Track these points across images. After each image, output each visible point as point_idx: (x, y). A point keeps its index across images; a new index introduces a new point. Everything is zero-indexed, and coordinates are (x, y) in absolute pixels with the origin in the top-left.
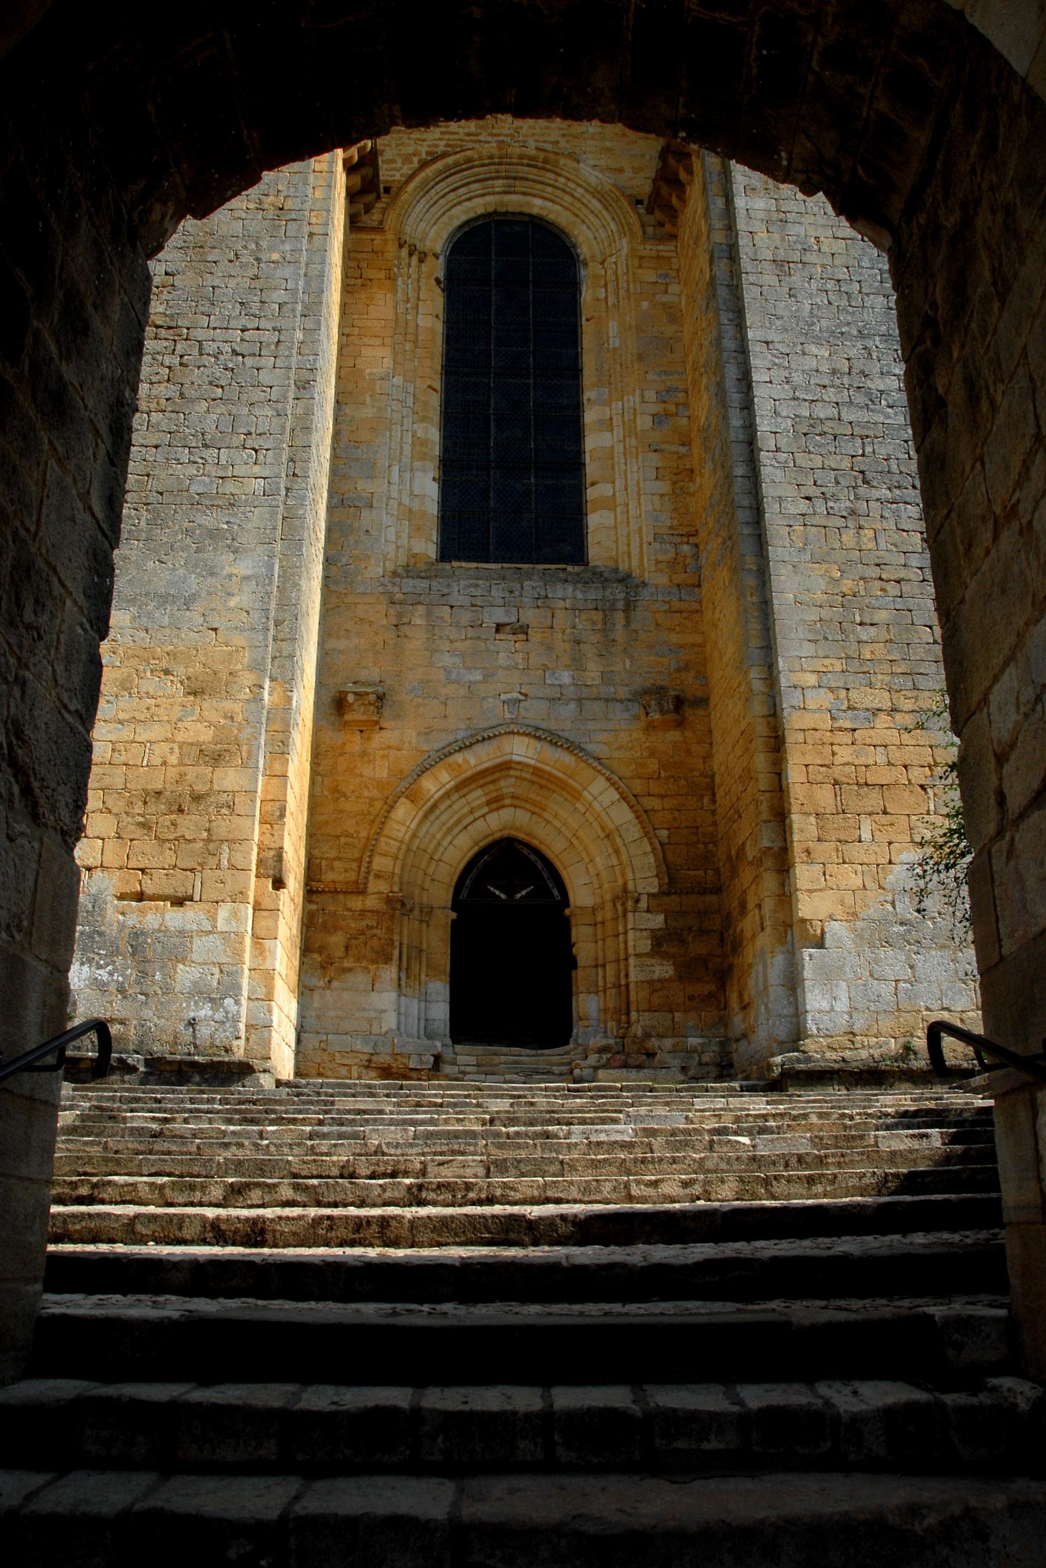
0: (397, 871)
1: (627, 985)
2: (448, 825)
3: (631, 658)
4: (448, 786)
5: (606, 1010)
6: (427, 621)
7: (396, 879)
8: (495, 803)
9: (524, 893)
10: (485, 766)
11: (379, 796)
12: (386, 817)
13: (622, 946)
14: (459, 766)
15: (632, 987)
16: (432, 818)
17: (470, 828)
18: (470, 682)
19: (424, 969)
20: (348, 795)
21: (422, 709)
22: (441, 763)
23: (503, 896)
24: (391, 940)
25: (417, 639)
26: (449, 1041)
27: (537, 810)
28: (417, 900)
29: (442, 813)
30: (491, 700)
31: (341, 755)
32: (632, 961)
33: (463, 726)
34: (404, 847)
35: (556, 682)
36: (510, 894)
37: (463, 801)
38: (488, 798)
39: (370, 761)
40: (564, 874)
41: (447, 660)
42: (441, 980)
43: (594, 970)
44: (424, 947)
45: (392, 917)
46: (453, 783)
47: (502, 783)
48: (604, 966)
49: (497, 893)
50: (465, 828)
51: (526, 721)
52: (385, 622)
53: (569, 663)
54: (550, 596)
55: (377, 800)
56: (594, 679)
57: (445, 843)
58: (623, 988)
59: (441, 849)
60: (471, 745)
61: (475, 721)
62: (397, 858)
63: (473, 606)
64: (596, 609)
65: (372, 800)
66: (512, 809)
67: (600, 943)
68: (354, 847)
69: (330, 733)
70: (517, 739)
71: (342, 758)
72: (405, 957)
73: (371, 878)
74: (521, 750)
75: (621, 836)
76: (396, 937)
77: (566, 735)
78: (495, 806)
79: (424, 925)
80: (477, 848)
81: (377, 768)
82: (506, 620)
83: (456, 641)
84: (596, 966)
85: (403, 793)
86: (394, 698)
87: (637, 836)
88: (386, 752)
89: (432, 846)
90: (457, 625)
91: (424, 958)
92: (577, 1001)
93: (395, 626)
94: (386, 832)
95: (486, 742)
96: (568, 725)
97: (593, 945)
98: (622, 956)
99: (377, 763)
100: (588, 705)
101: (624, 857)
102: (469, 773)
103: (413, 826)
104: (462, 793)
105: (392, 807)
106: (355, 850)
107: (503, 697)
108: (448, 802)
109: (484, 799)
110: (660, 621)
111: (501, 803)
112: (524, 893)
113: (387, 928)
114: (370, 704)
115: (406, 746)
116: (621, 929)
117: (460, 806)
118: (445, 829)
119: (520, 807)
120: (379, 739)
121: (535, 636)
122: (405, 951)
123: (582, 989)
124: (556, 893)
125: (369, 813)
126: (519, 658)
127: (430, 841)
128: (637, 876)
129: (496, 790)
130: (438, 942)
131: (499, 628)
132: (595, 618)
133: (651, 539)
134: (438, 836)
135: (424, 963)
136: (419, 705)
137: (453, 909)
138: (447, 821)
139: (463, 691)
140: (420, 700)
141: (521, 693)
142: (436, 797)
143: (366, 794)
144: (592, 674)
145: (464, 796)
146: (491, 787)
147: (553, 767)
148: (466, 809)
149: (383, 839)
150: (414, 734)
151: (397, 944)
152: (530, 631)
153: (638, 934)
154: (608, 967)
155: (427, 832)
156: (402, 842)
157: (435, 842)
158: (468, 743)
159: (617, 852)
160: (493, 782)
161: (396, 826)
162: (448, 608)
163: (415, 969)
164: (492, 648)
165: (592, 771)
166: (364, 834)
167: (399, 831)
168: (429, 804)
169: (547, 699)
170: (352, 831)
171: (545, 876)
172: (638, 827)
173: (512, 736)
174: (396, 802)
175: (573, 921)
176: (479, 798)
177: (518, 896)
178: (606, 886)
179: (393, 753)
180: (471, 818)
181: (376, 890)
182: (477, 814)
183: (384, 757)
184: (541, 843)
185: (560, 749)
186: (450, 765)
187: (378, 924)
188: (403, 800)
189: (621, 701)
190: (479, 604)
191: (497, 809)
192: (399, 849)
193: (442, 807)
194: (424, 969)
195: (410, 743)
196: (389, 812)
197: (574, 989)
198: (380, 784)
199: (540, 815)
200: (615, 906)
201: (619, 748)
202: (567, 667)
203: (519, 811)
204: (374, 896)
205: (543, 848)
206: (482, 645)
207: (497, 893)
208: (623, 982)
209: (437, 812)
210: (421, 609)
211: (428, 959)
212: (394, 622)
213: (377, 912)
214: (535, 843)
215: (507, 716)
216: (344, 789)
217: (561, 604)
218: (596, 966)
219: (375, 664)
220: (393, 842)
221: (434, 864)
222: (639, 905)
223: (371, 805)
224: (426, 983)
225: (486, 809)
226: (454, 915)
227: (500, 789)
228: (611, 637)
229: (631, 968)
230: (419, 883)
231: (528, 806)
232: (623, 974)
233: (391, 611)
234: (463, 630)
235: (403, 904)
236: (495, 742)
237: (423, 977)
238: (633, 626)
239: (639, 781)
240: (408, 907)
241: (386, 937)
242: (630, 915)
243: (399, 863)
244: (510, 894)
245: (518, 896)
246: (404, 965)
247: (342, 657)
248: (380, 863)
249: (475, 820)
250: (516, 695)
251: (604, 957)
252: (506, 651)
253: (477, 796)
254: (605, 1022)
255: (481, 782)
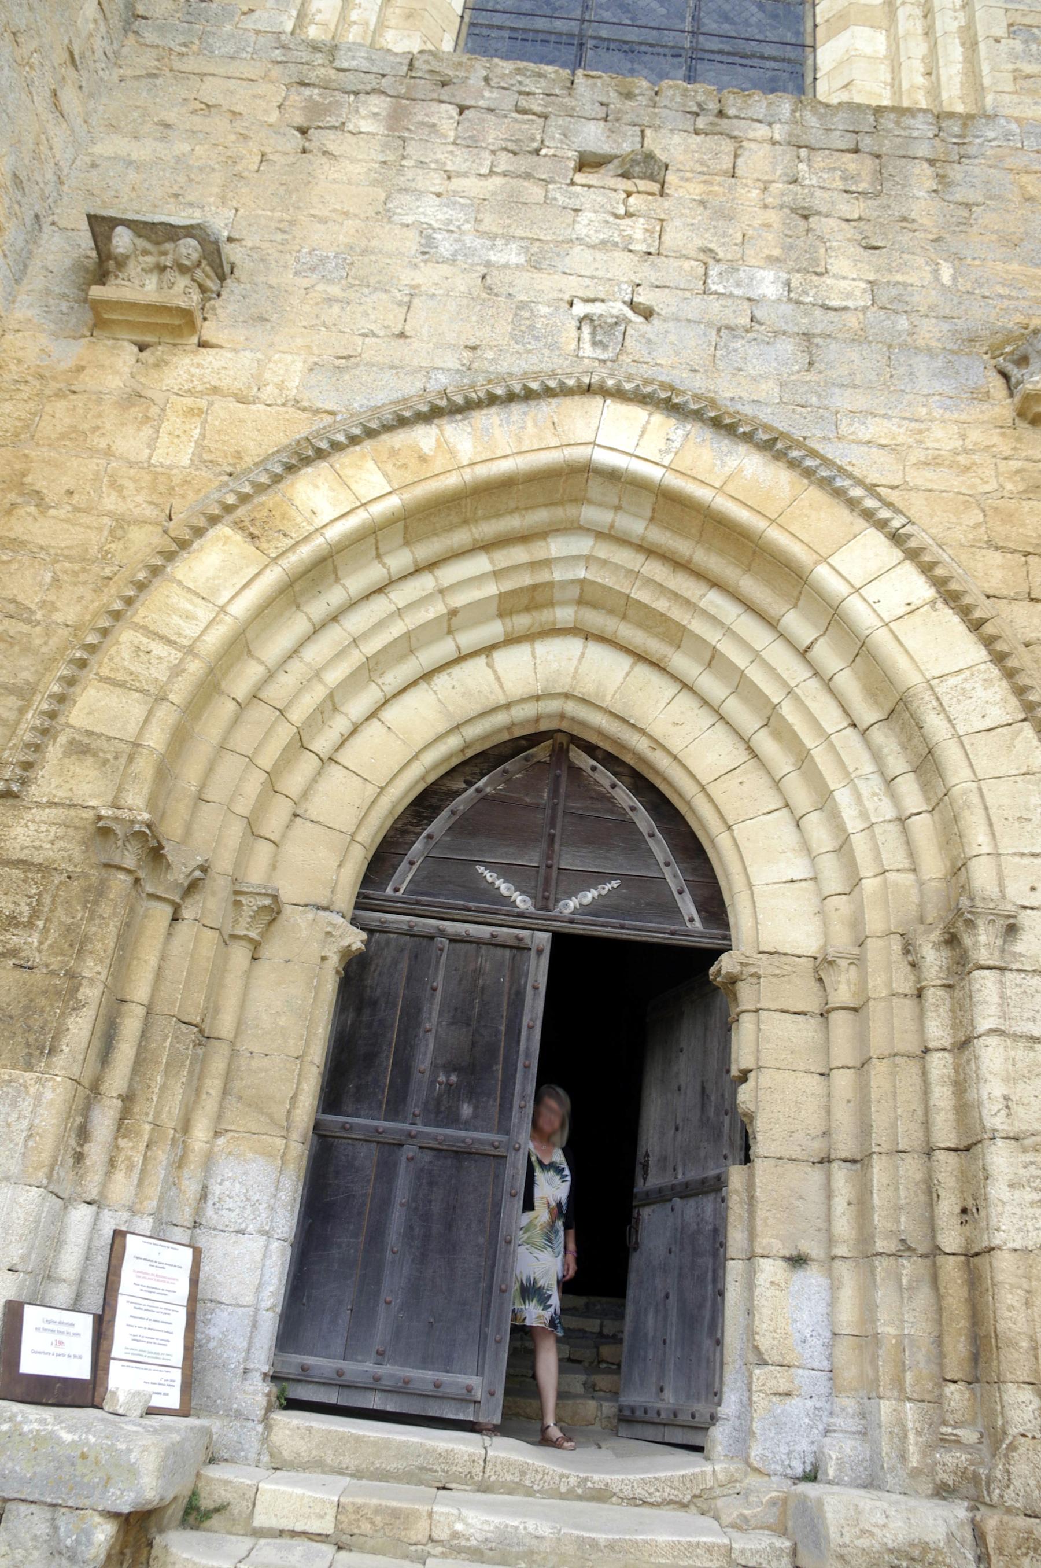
0: (156, 738)
1: (975, 1257)
2: (372, 646)
3: (956, 259)
4: (378, 510)
5: (868, 1339)
6: (391, 129)
7: (144, 766)
8: (527, 611)
9: (589, 896)
10: (505, 466)
11: (150, 512)
12: (156, 571)
13: (942, 1096)
14: (423, 459)
15: (1004, 1267)
16: (318, 608)
17: (441, 681)
18: (488, 264)
19: (210, 1104)
20: (50, 497)
21: (336, 309)
22: (368, 445)
23: (522, 902)
24: (72, 976)
25: (354, 161)
26: (256, 1393)
27: (654, 646)
28: (223, 863)
29: (352, 605)
30: (544, 310)
31: (59, 394)
32: (1000, 1159)
33: (451, 361)
34: (195, 667)
35: (738, 292)
36: (545, 903)
37: (426, 583)
38: (507, 585)
39: (147, 419)
40: (722, 849)
41: (431, 212)
42: (267, 1153)
43: (816, 1175)
44: (225, 1025)
45: (99, 891)
46: (393, 502)
47: (556, 547)
48: (859, 1162)
49: (504, 887)
50: (427, 676)
51: (646, 371)
52: (274, 117)
53: (777, 252)
54: (731, 111)
55: (141, 522)
56: (849, 295)
57: (357, 707)
58: (951, 1268)
59: (340, 725)
60: (470, 406)
61: (490, 355)
62: (161, 698)
63: (519, 111)
64: (856, 151)
65: (121, 524)
66: (573, 646)
67: (843, 1080)
68: (26, 650)
69: (44, 340)
70: (614, 408)
71: (61, 405)
72: (125, 1052)
73: (54, 752)
74: (625, 438)
75: (942, 709)
76: (94, 969)
77: (765, 415)
78: (522, 622)
79: (240, 955)
80: (454, 742)
81: (164, 439)
82: (606, 148)
83: (465, 175)
84: (826, 1160)
85: (228, 509)
86: (260, 279)
87: (997, 715)
88: (203, 403)
89: (309, 702)
90: (472, 144)
91: (218, 1065)
92: (750, 1286)
93: (303, 131)
94: (142, 613)
95: (517, 410)
96: (768, 390)
97: (814, 1083)
98: (945, 1133)
99: (166, 427)
100: (832, 351)
101: (958, 775)
102: (451, 481)
103: (241, 608)
104: (426, 551)
105: (184, 545)
106: (24, 662)
107: (580, 309)
108: (373, 574)
109: (491, 589)
110: (1032, 191)
111: (545, 616)
112: (589, 896)
113: (68, 930)
114: (183, 269)
115: (269, 392)
116: (938, 1031)
117: (418, 601)
118: (356, 658)
119: (602, 639)
120: (186, 368)
121: (683, 189)
122: (131, 1026)
123: (769, 1240)
124: (688, 907)
125: (105, 556)
126: (637, 230)
127: (304, 686)
128: (1007, 846)
129: (534, 565)
130: (283, 1019)
131: (587, 163)
132: (852, 167)
133: (1000, 31)
134: (334, 676)
135: (213, 1085)
136: (330, 300)
137: (354, 921)
138: (366, 635)
139: (464, 282)
140: (335, 290)
141: (631, 304)
142: (334, 533)
143: (110, 502)
144: (843, 284)
145: (431, 566)
146: (519, 554)
147: (720, 489)
148: (437, 609)
149: (127, 637)
150: (299, 366)
151: (91, 993)
152: (671, 177)
153: (1020, 1052)
154: (879, 1171)
155: (295, 652)
156: (190, 651)
157: (319, 693)
158: (459, 400)
159: (927, 764)
160: (524, 538)
161: (184, 604)
162: (454, 111)
163: (164, 1098)
164: (561, 200)
165: (844, 513)
166: (68, 613)
167: (188, 617)
168: (306, 552)
169: (709, 324)
170: (32, 599)
171: (661, 861)
172: (1001, 688)
173: (598, 400)
174: (199, 532)
175: (746, 995)
176: (478, 579)
177: (570, 905)
178: (870, 885)
179: (223, 409)
180: (445, 649)
181: (61, 794)
182: (469, 639)
183: (192, 412)
184: (657, 744)
185: (742, 448)
186: (393, 453)
187: (35, 914)
188: (223, 530)
189: (930, 352)
190: (537, 109)
191: (529, 637)
192: (177, 671)
193: (356, 582)
194: (210, 1104)
195: (281, 387)
196: (170, 556)
197: (736, 1238)
198: (161, 482)
199: (658, 666)
200: (907, 949)
201: (934, 462)
202: (772, 260)
203: (596, 652)
204: (48, 813)
205: (662, 761)
206: (534, 192)
207: (504, 887)
208: (951, 1239)
209: (335, 596)
210: (378, 104)
211: (228, 1077)
212: (299, 120)
213: (45, 869)
214: (641, 744)
215: (587, 349)
216: (41, 485)
217: (762, 131)
218: (826, 1160)
219: (224, 200)
220: (158, 649)
221: (307, 764)
222: (1019, 947)
223: (113, 535)
224: (208, 1161)
225: (495, 630)
226: (356, 939)
227: (547, 563)
228: (897, 210)
229: (998, 1190)
230: (243, 807)
231: (627, 632)
232: (948, 1206)
233: (298, 97)
234: (486, 154)
235: (156, 855)
236: (547, 408)
237: (201, 1132)
238: (960, 194)
239: (998, 557)
240: (179, 874)
241: (55, 962)
242: (986, 984)
243: (166, 716)
244: (545, 903)
245: (570, 905)
246: (117, 1080)
247: (132, 176)
248: (94, 708)
249: (461, 658)
250: (618, 308)
251: (865, 1129)
252: (597, 201)
253: (473, 579)
254: (872, 1391)
255: (488, 529)
